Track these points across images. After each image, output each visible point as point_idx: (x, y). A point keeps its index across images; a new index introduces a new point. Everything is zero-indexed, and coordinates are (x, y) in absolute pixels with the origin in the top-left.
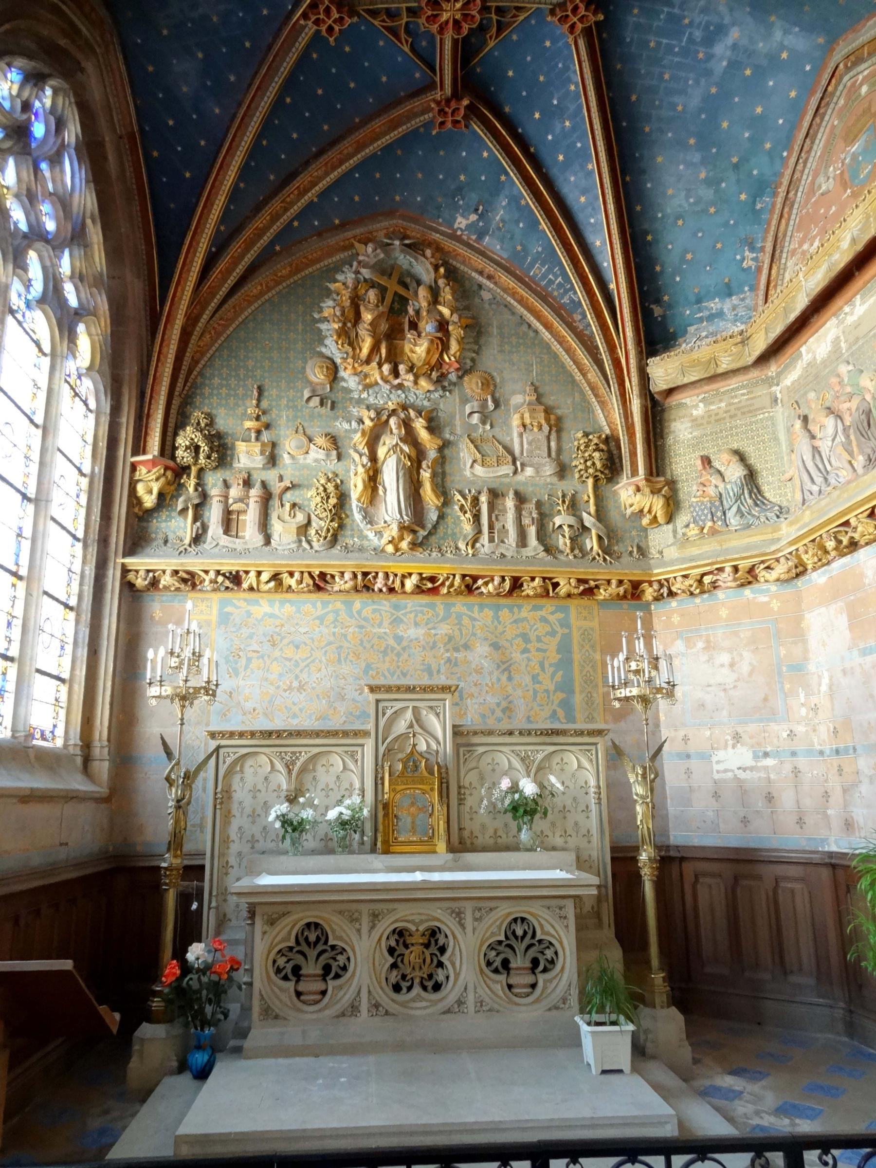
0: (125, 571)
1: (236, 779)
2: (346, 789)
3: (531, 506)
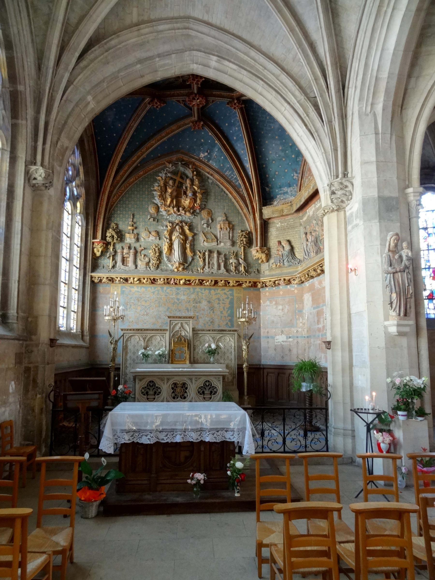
0: (92, 277)
1: (129, 342)
2: (161, 345)
3: (222, 256)
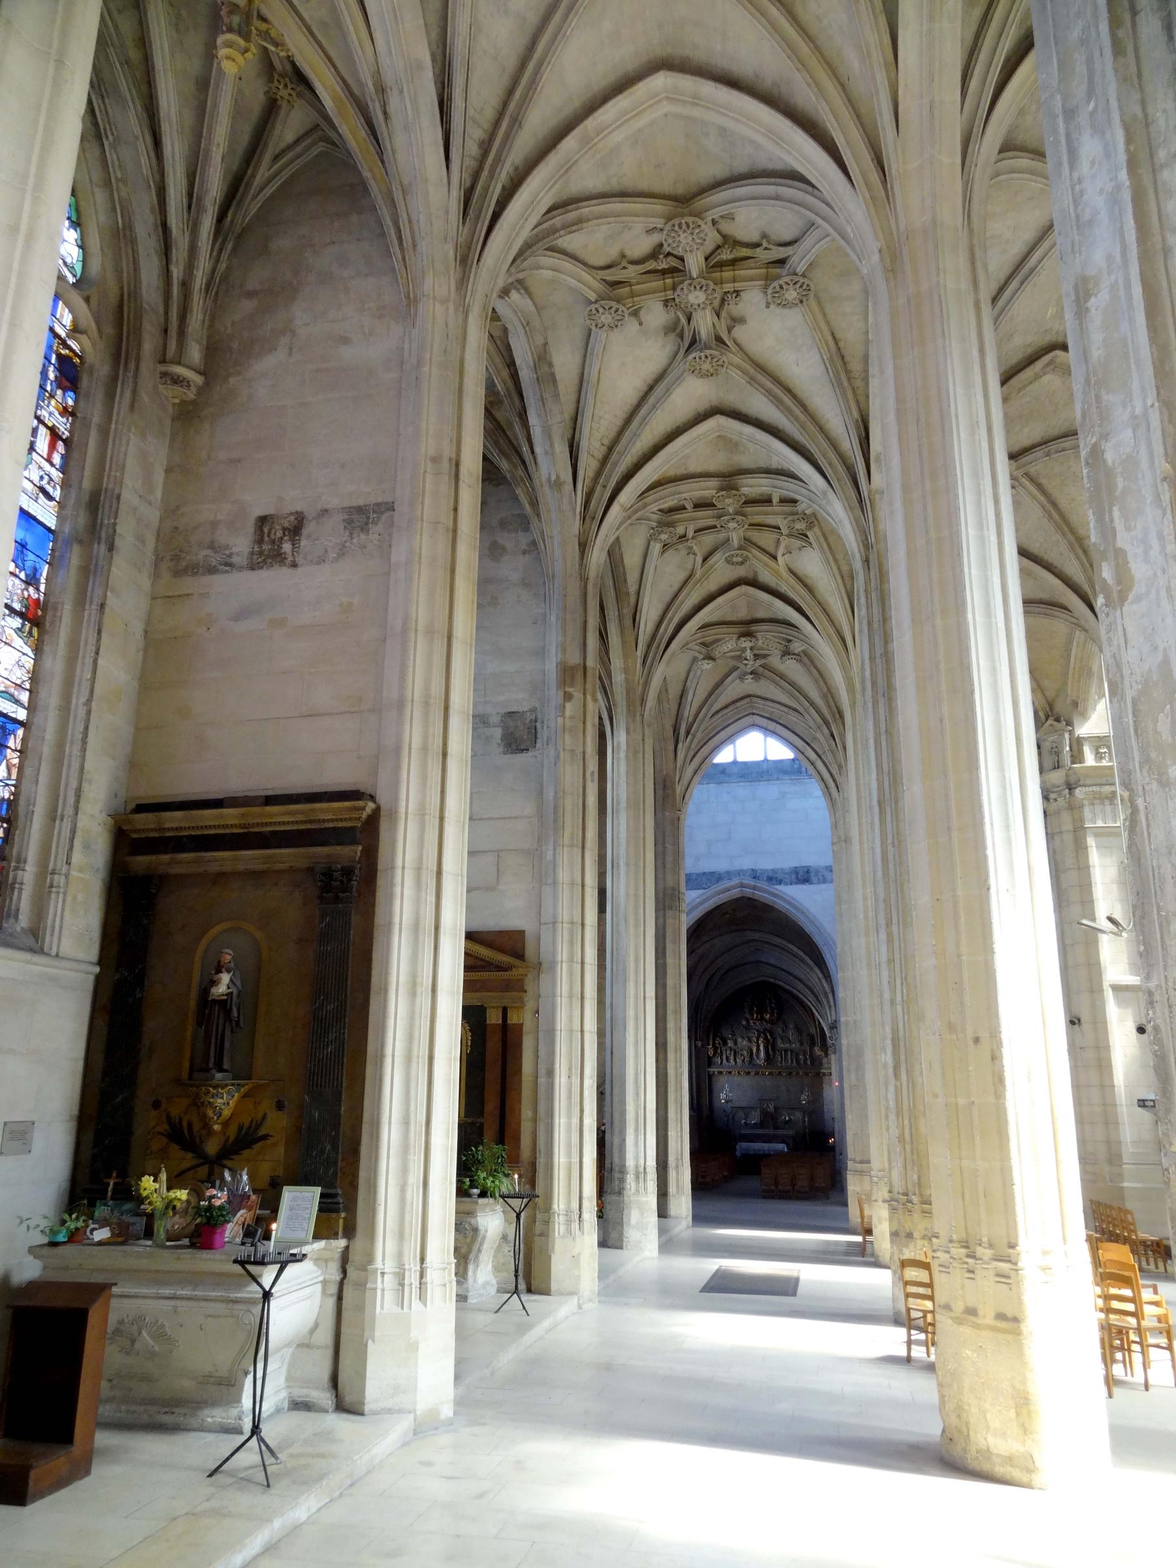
2: (755, 1118)
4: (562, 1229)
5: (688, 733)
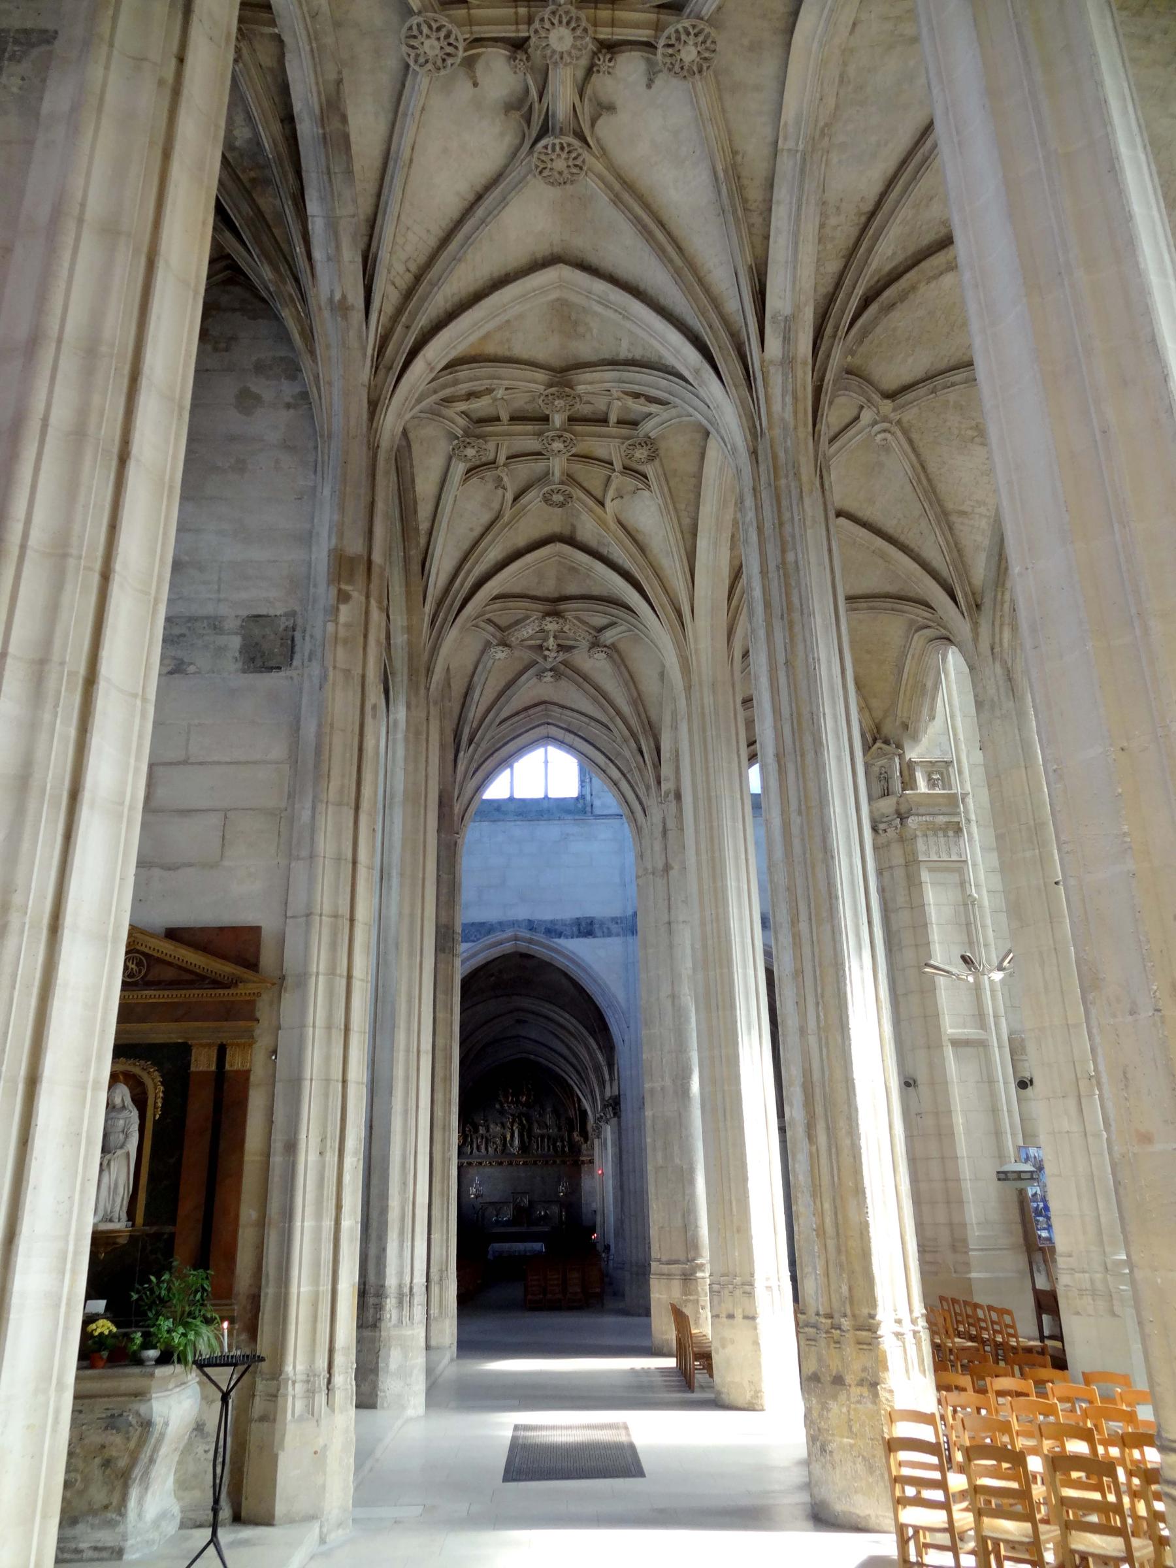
2: (507, 1214)
4: (300, 1405)
5: (471, 741)
